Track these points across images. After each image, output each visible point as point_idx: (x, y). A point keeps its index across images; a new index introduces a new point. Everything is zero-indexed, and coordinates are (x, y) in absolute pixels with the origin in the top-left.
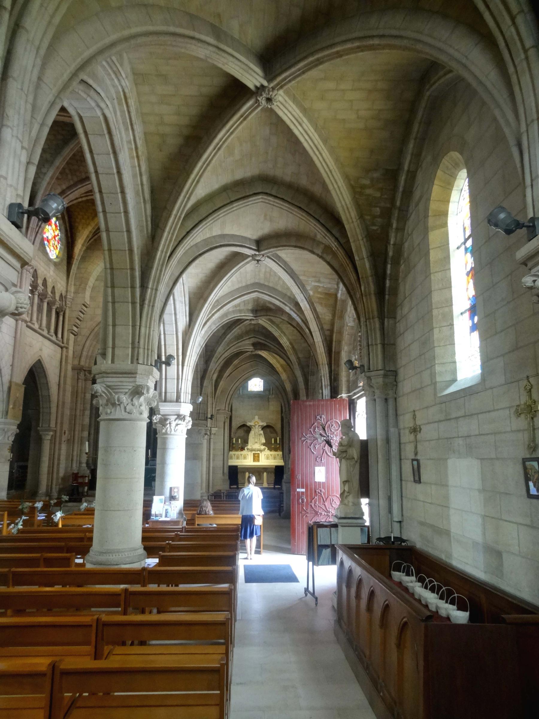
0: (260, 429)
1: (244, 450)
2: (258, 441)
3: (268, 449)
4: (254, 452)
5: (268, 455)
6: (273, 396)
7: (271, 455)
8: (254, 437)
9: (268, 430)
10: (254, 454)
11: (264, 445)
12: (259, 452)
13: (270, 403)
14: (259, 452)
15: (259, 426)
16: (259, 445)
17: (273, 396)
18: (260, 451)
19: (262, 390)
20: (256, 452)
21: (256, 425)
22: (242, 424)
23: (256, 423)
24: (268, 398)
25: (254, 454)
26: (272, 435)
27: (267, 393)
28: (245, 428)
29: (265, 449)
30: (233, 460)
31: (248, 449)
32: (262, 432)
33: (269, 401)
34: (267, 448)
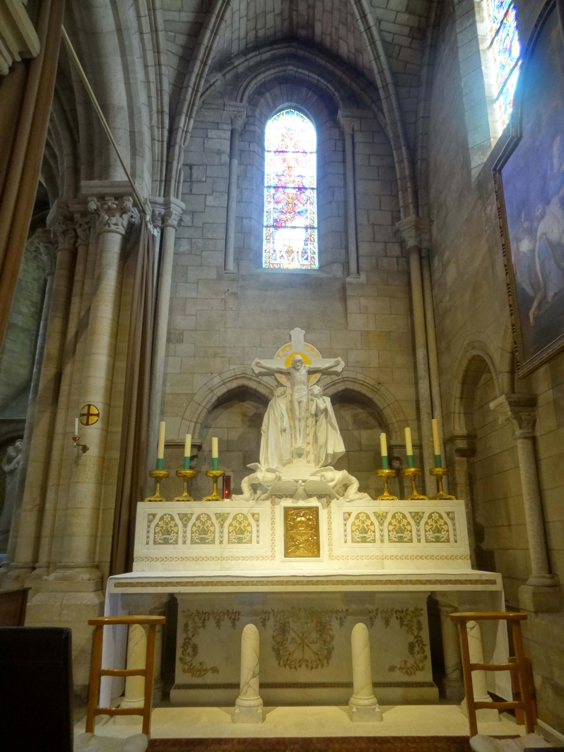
0: (317, 389)
1: (240, 492)
2: (309, 448)
3: (361, 489)
4: (288, 503)
5: (362, 517)
6: (363, 277)
7: (381, 517)
8: (286, 423)
9: (348, 414)
10: (287, 510)
11: (338, 466)
12: (314, 502)
13: (352, 305)
14: (314, 502)
15: (311, 372)
16: (313, 468)
17: (363, 277)
18: (320, 497)
19: (316, 265)
20: (302, 503)
21: (296, 365)
22: (234, 384)
23: (299, 357)
24: (344, 289)
25: (287, 510)
26: (365, 435)
27: (338, 270)
28: (249, 407)
29: (346, 487)
30: (181, 549)
31: (255, 488)
32: (326, 403)
33: (344, 299)
34: (355, 484)
